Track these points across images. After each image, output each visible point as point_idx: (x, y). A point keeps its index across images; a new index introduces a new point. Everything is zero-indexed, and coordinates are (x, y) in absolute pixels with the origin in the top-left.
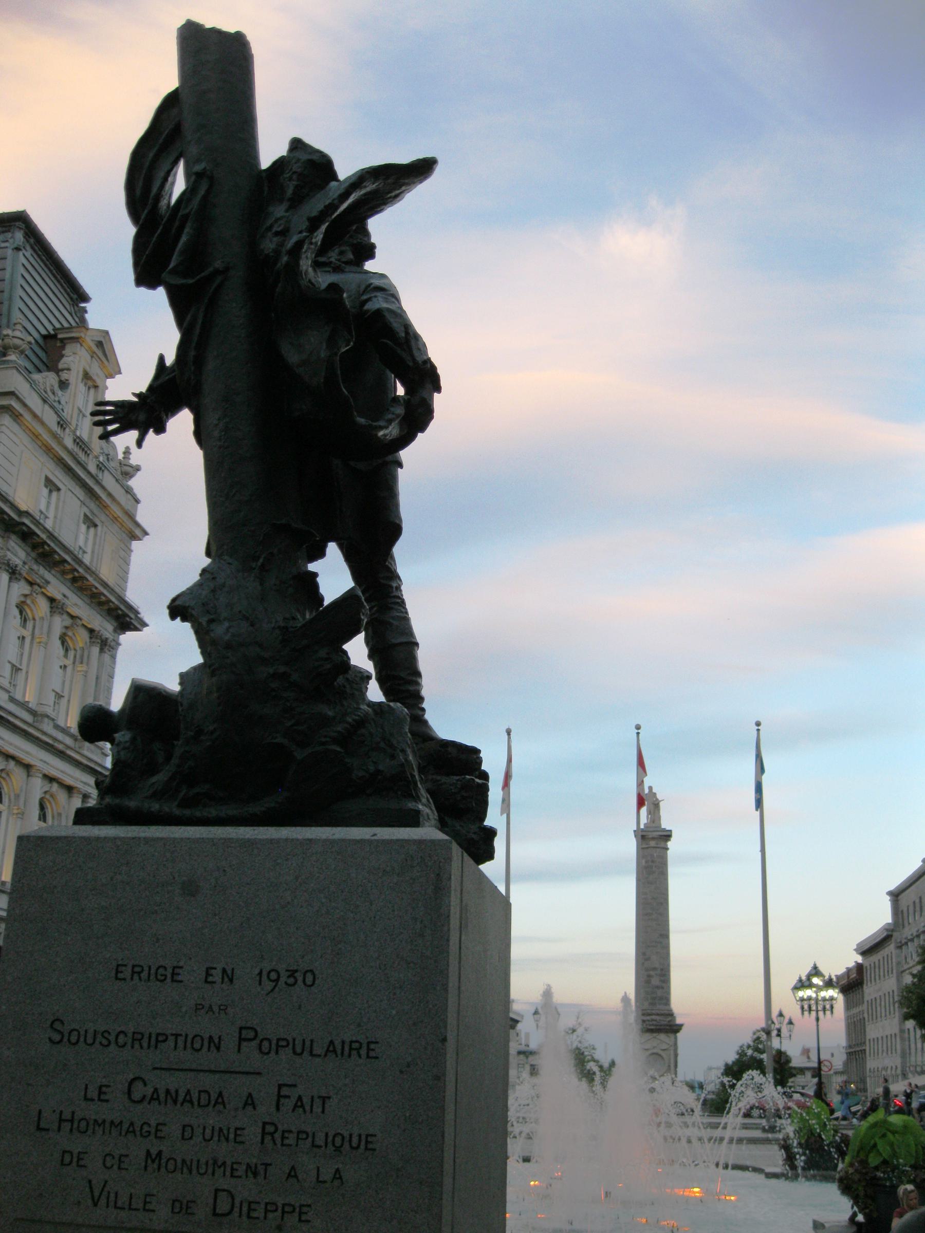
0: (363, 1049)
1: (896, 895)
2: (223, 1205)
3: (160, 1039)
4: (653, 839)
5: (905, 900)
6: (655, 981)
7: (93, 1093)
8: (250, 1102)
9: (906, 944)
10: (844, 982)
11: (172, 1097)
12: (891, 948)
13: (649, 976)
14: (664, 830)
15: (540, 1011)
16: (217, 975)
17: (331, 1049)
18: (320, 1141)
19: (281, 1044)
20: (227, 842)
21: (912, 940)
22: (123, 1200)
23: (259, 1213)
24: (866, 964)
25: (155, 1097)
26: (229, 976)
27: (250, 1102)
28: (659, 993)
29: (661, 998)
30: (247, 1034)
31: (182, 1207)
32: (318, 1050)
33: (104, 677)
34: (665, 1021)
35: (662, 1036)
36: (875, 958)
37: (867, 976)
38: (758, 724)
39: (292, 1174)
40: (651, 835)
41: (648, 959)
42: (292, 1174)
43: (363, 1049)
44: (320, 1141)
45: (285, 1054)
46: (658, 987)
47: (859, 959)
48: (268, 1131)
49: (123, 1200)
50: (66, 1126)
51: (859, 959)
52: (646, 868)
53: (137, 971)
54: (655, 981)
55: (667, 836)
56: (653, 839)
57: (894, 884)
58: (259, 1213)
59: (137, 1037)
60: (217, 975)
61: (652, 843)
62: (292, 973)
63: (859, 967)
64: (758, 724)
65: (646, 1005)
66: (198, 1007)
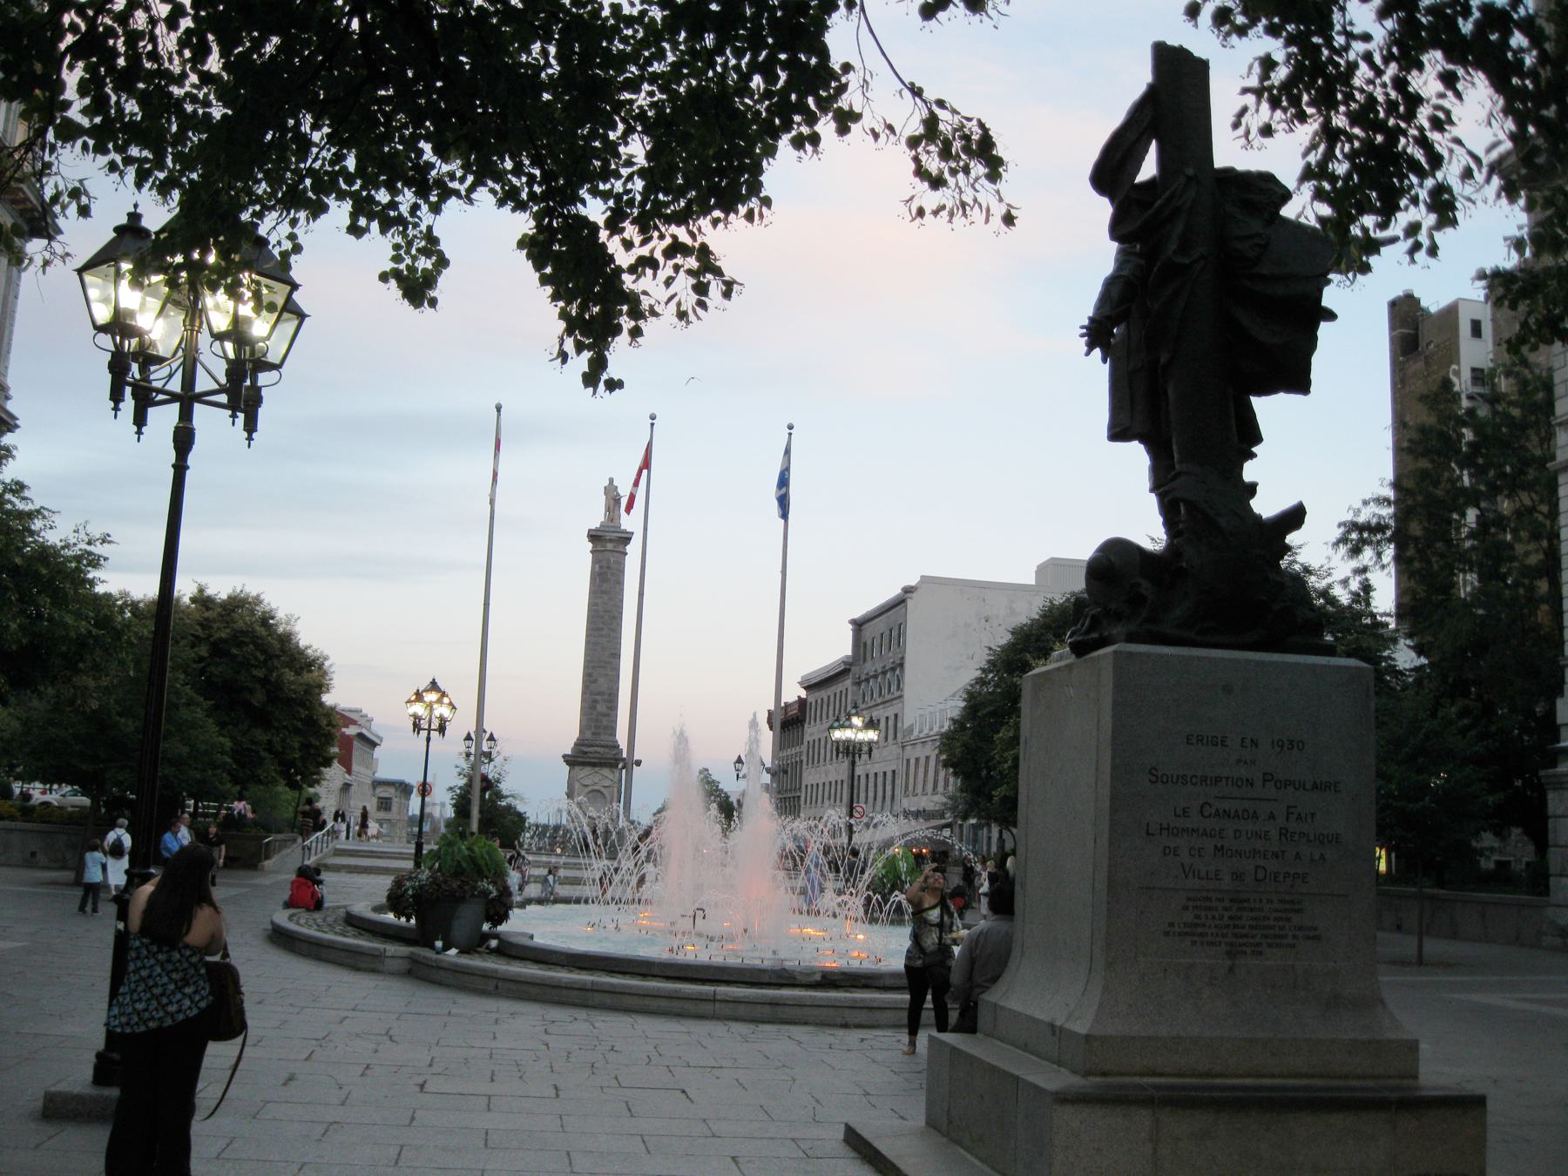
0: (1331, 787)
1: (859, 625)
2: (1261, 875)
3: (1218, 780)
4: (611, 541)
5: (870, 631)
6: (601, 708)
7: (1179, 812)
8: (1272, 816)
9: (867, 680)
11: (1227, 814)
12: (848, 683)
13: (596, 701)
14: (625, 532)
16: (1248, 742)
17: (1315, 786)
18: (1312, 837)
19: (1287, 783)
20: (1248, 661)
21: (875, 677)
22: (1203, 874)
23: (1281, 878)
24: (811, 699)
25: (1217, 814)
26: (1254, 743)
27: (1272, 816)
28: (605, 721)
29: (606, 728)
30: (1267, 778)
31: (1238, 876)
32: (1308, 786)
33: (11, 298)
34: (611, 754)
35: (606, 771)
36: (823, 694)
37: (810, 714)
38: (791, 427)
39: (1298, 856)
40: (609, 536)
41: (595, 681)
42: (1298, 856)
43: (1331, 787)
44: (1312, 837)
45: (1290, 789)
46: (604, 715)
47: (803, 694)
48: (1283, 832)
49: (1203, 874)
50: (1165, 833)
51: (803, 694)
52: (600, 574)
53: (1200, 739)
54: (601, 708)
56: (611, 541)
57: (858, 613)
58: (1281, 878)
59: (1204, 779)
60: (1248, 742)
61: (610, 546)
62: (1291, 742)
63: (802, 703)
64: (791, 427)
65: (588, 735)
66: (1239, 761)
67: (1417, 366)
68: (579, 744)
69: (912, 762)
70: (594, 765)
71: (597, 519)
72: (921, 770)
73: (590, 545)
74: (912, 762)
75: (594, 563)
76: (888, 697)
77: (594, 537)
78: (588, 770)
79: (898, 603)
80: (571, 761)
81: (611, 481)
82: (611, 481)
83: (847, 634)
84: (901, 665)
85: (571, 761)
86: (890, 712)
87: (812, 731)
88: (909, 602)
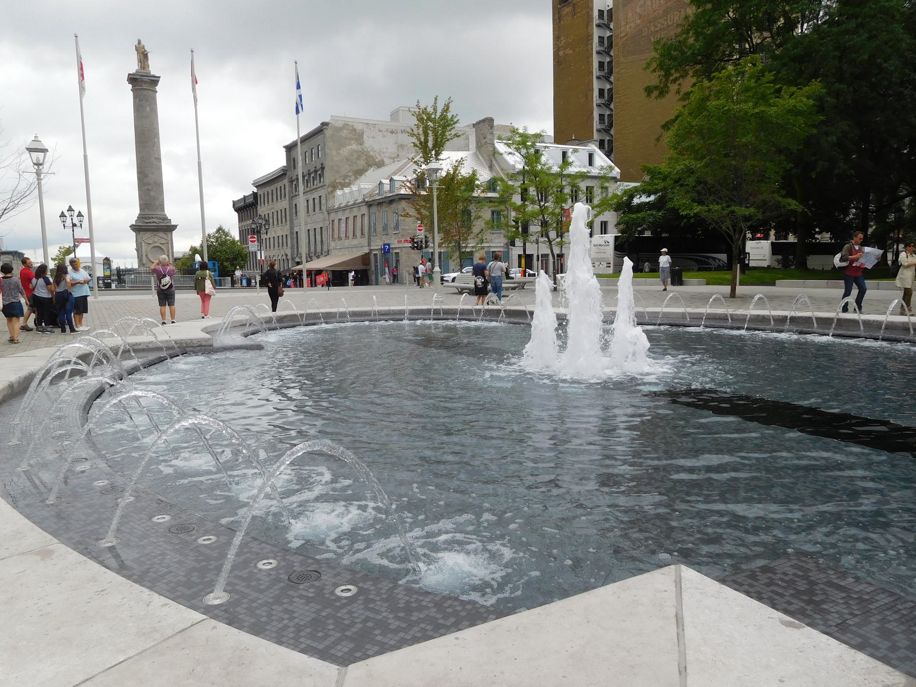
1: (290, 149)
10: (242, 204)
12: (286, 181)
15: (66, 213)
35: (161, 234)
47: (255, 190)
51: (255, 190)
55: (155, 81)
63: (255, 195)
67: (567, 10)
68: (141, 217)
69: (336, 222)
70: (154, 230)
71: (133, 67)
72: (343, 225)
73: (130, 86)
74: (336, 222)
75: (135, 97)
76: (313, 187)
77: (133, 79)
78: (148, 234)
79: (318, 132)
80: (136, 228)
81: (139, 42)
82: (139, 42)
83: (283, 153)
84: (323, 168)
85: (136, 228)
86: (316, 195)
87: (262, 210)
88: (325, 131)
